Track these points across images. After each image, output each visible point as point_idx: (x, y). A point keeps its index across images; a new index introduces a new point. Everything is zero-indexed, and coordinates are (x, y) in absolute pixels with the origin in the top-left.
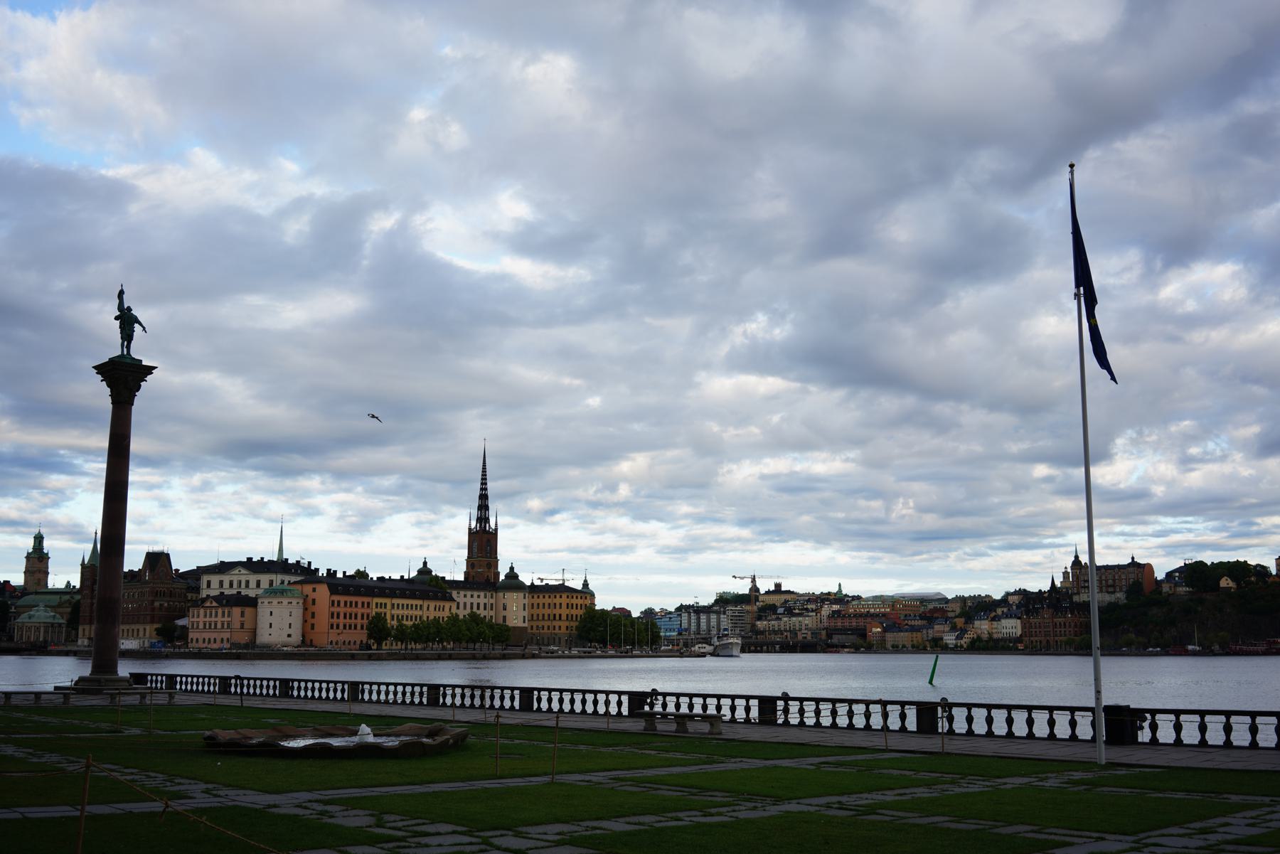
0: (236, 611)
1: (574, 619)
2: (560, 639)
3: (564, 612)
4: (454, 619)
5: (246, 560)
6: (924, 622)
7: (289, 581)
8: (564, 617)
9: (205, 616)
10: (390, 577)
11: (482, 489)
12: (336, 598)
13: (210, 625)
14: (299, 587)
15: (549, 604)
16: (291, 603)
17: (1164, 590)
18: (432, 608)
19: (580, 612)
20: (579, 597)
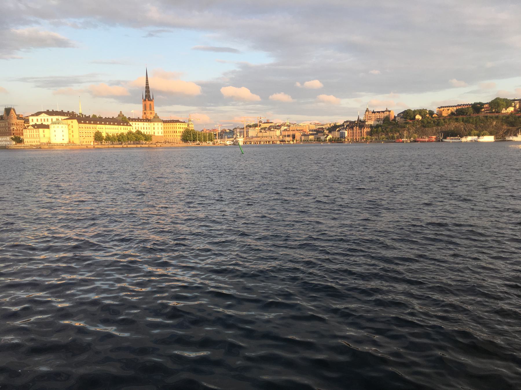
0: (41, 130)
4: (130, 133)
6: (315, 132)
8: (178, 132)
9: (29, 133)
12: (81, 125)
13: (32, 136)
14: (66, 121)
17: (396, 120)
18: (122, 129)
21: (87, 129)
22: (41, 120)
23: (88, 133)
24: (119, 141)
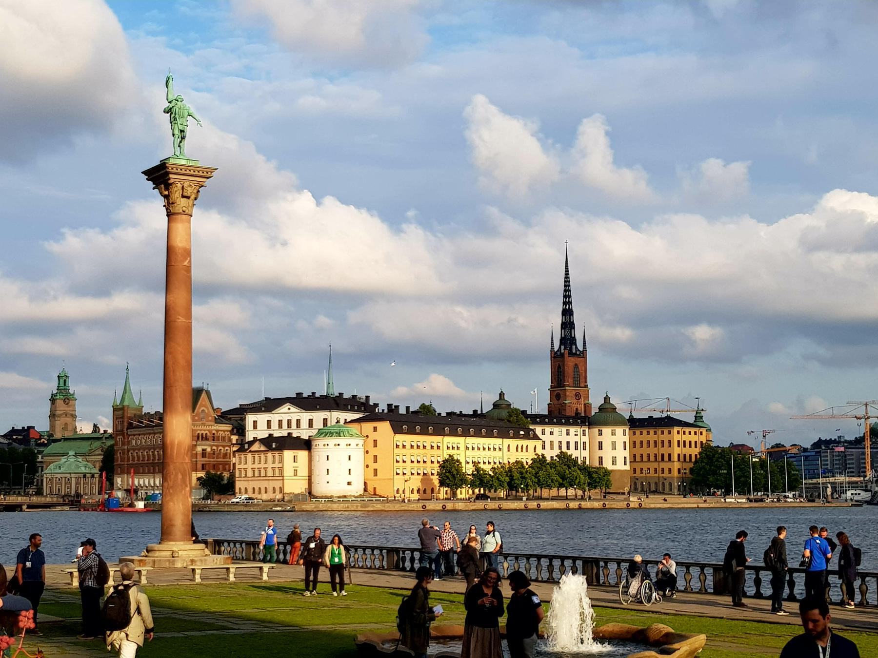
0: (288, 454)
1: (688, 459)
2: (670, 484)
3: (677, 451)
4: (540, 461)
5: (295, 396)
7: (346, 420)
10: (461, 412)
11: (564, 303)
12: (401, 438)
13: (260, 471)
15: (655, 442)
16: (350, 445)
19: (695, 451)
20: (693, 433)
21: (415, 451)
22: (280, 422)
23: (418, 462)
24: (512, 486)
